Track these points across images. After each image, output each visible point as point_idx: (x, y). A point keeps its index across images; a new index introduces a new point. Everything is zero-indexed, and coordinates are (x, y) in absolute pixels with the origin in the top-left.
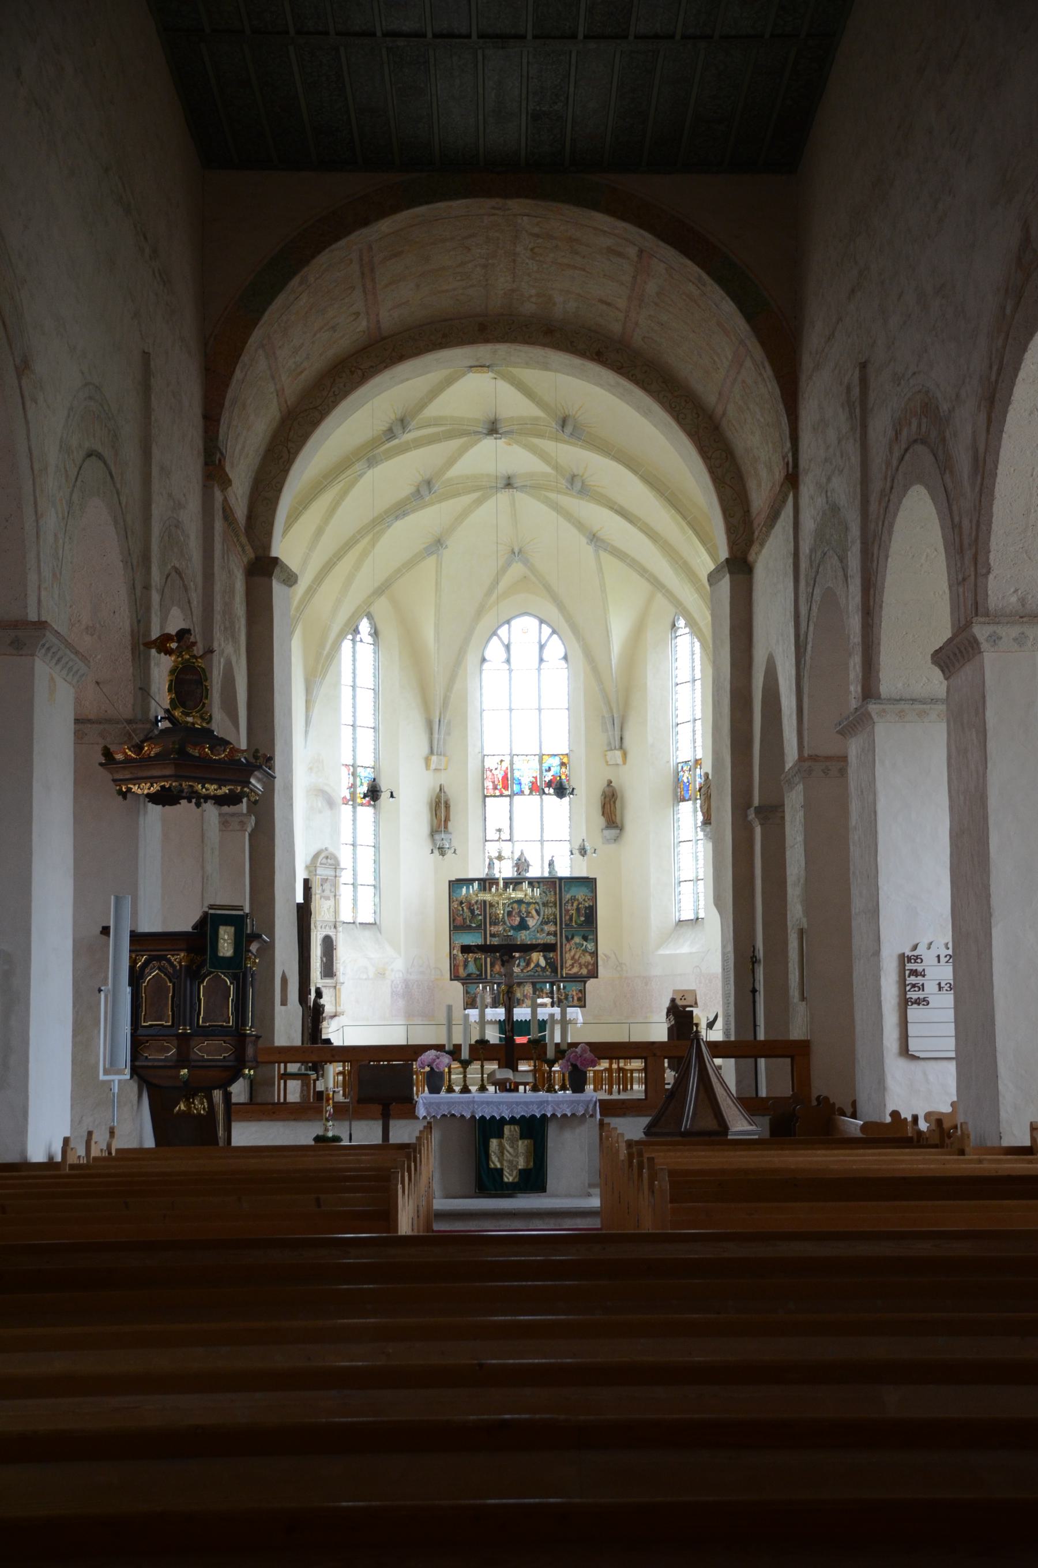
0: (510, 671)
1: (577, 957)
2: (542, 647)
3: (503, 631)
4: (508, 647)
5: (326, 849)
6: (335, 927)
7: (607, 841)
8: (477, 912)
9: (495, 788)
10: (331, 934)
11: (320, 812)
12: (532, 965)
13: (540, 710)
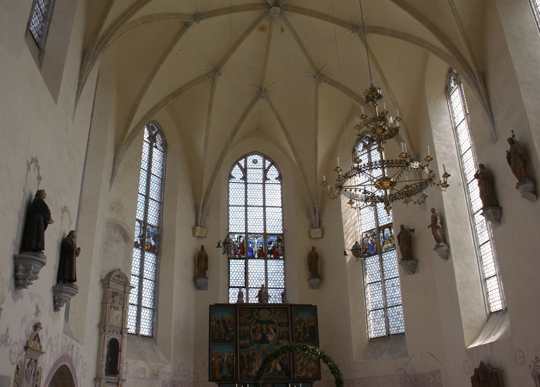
0: (246, 184)
1: (305, 364)
2: (265, 171)
3: (242, 162)
4: (244, 170)
5: (119, 270)
6: (121, 333)
7: (312, 287)
8: (230, 329)
9: (236, 253)
10: (117, 338)
11: (117, 241)
12: (271, 370)
13: (264, 207)
